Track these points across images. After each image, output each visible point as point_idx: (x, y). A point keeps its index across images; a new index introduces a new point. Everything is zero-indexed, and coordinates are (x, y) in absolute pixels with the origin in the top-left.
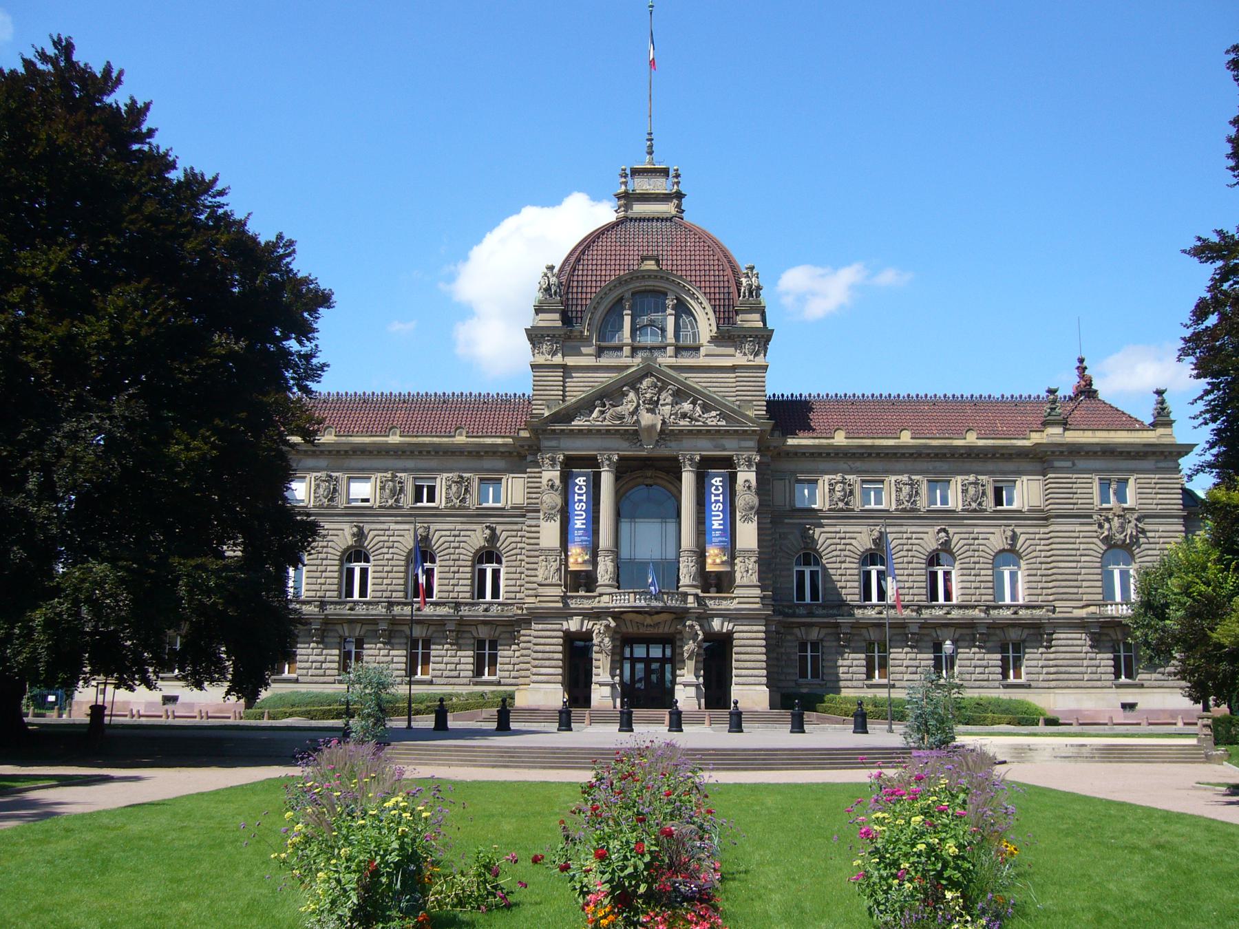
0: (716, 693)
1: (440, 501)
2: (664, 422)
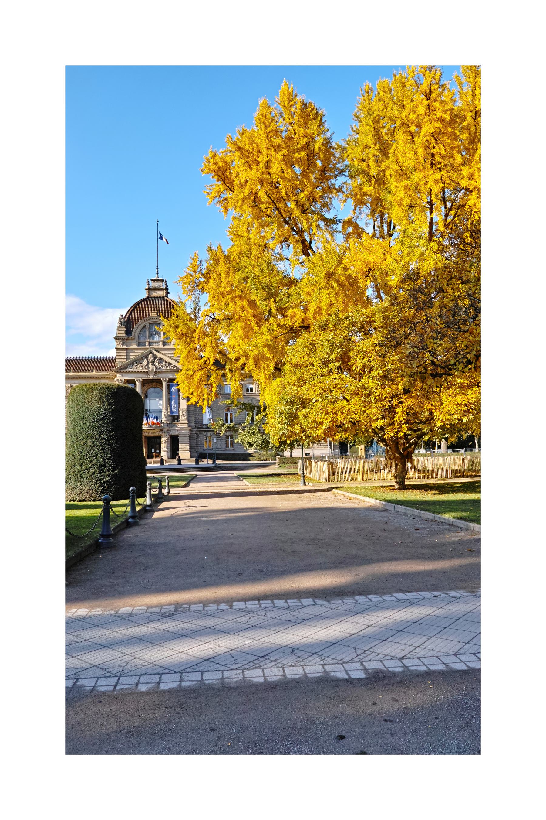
0: (174, 452)
2: (156, 368)
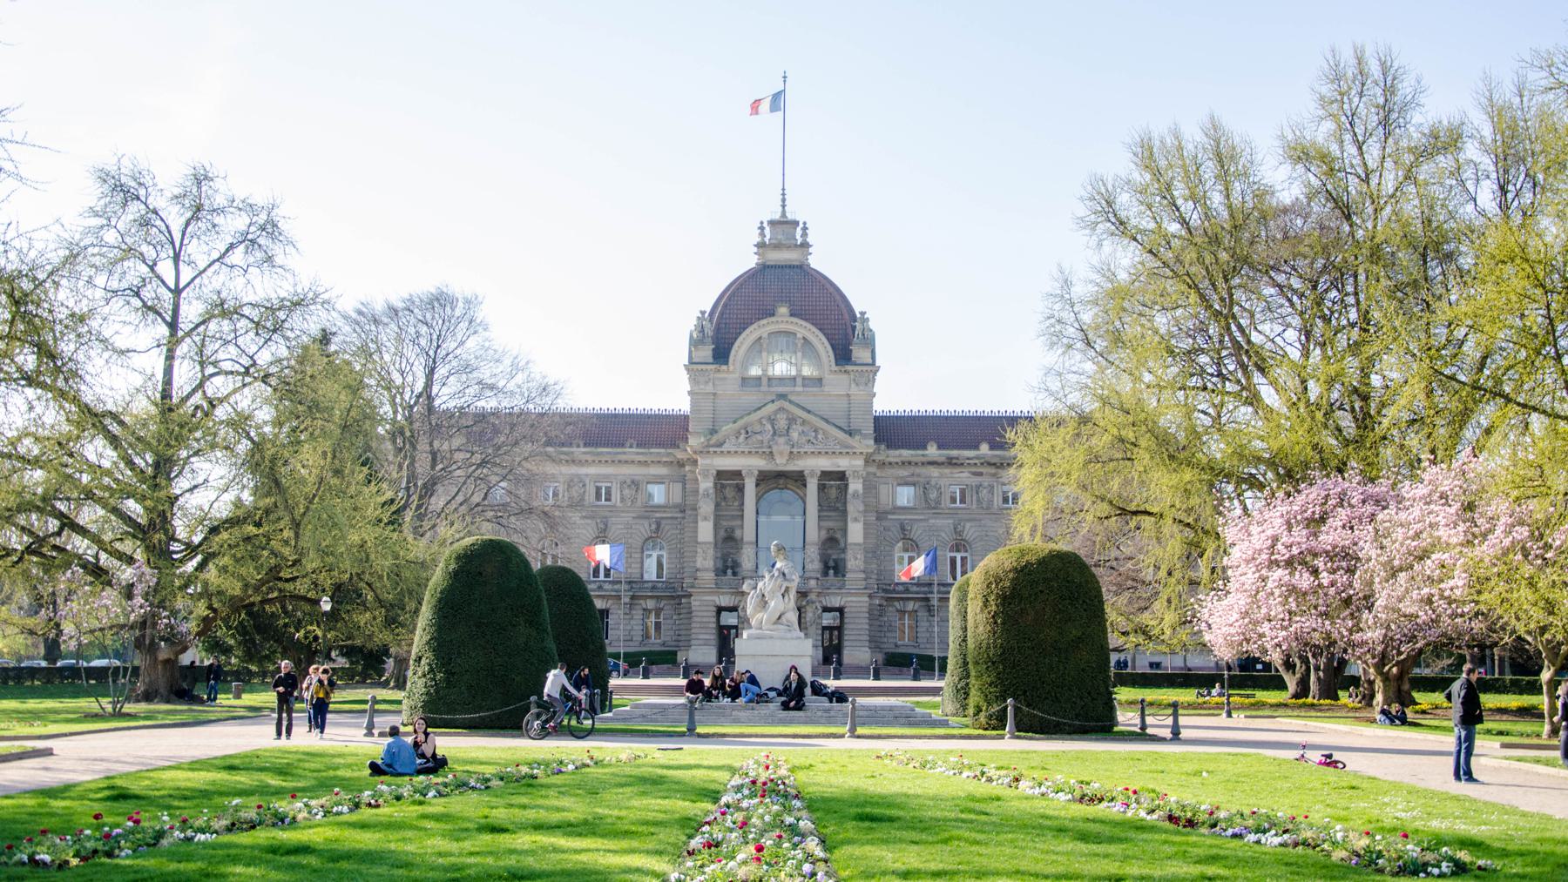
1: (616, 496)
